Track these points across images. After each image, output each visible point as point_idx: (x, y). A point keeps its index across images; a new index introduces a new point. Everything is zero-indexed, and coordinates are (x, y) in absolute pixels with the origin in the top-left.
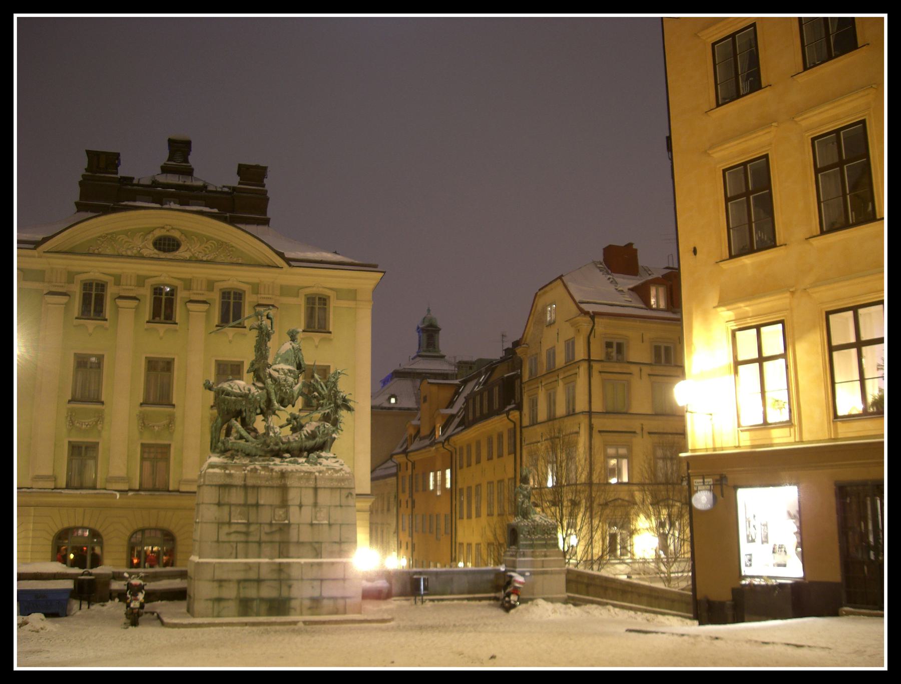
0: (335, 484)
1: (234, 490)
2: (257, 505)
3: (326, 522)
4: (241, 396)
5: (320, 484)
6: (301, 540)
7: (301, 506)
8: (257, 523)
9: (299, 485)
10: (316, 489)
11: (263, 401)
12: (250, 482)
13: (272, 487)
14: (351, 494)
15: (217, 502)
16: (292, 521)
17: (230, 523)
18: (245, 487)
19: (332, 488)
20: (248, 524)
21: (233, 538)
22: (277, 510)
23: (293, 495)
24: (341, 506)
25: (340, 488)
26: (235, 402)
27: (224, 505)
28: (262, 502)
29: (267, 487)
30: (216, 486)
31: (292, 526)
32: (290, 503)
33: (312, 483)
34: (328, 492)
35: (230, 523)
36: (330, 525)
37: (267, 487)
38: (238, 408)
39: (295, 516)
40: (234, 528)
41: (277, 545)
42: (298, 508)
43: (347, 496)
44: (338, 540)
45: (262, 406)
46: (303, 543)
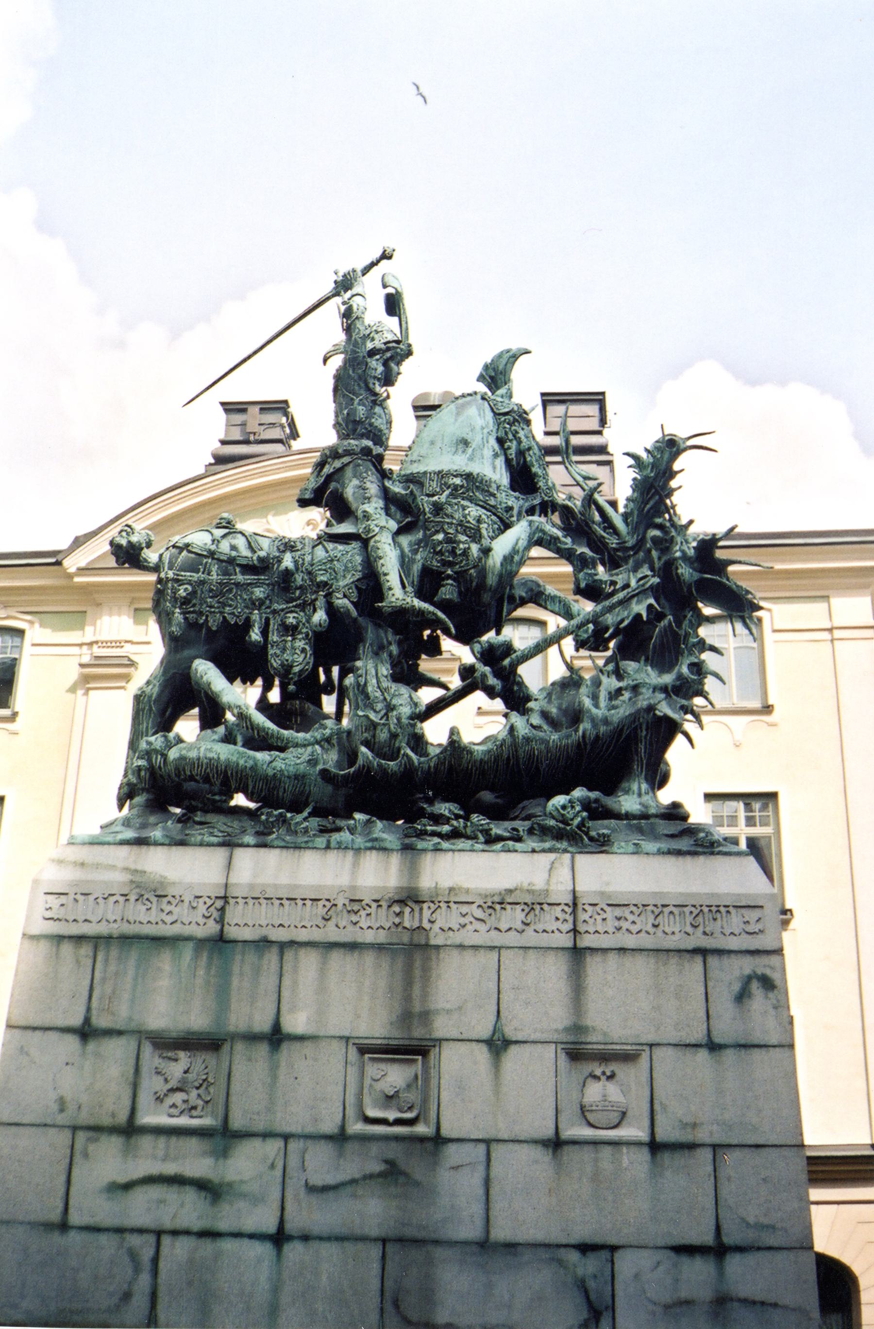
1: (165, 961)
2: (276, 1037)
3: (642, 1135)
4: (248, 569)
6: (501, 1232)
7: (498, 1044)
9: (497, 939)
11: (345, 581)
12: (243, 924)
15: (76, 1020)
17: (130, 1130)
21: (141, 1208)
22: (373, 1070)
23: (459, 993)
25: (703, 952)
26: (221, 592)
30: (79, 939)
33: (554, 930)
38: (234, 612)
39: (466, 1093)
40: (150, 1158)
41: (375, 1252)
42: (482, 1054)
44: (707, 1238)
45: (340, 602)
46: (511, 1247)
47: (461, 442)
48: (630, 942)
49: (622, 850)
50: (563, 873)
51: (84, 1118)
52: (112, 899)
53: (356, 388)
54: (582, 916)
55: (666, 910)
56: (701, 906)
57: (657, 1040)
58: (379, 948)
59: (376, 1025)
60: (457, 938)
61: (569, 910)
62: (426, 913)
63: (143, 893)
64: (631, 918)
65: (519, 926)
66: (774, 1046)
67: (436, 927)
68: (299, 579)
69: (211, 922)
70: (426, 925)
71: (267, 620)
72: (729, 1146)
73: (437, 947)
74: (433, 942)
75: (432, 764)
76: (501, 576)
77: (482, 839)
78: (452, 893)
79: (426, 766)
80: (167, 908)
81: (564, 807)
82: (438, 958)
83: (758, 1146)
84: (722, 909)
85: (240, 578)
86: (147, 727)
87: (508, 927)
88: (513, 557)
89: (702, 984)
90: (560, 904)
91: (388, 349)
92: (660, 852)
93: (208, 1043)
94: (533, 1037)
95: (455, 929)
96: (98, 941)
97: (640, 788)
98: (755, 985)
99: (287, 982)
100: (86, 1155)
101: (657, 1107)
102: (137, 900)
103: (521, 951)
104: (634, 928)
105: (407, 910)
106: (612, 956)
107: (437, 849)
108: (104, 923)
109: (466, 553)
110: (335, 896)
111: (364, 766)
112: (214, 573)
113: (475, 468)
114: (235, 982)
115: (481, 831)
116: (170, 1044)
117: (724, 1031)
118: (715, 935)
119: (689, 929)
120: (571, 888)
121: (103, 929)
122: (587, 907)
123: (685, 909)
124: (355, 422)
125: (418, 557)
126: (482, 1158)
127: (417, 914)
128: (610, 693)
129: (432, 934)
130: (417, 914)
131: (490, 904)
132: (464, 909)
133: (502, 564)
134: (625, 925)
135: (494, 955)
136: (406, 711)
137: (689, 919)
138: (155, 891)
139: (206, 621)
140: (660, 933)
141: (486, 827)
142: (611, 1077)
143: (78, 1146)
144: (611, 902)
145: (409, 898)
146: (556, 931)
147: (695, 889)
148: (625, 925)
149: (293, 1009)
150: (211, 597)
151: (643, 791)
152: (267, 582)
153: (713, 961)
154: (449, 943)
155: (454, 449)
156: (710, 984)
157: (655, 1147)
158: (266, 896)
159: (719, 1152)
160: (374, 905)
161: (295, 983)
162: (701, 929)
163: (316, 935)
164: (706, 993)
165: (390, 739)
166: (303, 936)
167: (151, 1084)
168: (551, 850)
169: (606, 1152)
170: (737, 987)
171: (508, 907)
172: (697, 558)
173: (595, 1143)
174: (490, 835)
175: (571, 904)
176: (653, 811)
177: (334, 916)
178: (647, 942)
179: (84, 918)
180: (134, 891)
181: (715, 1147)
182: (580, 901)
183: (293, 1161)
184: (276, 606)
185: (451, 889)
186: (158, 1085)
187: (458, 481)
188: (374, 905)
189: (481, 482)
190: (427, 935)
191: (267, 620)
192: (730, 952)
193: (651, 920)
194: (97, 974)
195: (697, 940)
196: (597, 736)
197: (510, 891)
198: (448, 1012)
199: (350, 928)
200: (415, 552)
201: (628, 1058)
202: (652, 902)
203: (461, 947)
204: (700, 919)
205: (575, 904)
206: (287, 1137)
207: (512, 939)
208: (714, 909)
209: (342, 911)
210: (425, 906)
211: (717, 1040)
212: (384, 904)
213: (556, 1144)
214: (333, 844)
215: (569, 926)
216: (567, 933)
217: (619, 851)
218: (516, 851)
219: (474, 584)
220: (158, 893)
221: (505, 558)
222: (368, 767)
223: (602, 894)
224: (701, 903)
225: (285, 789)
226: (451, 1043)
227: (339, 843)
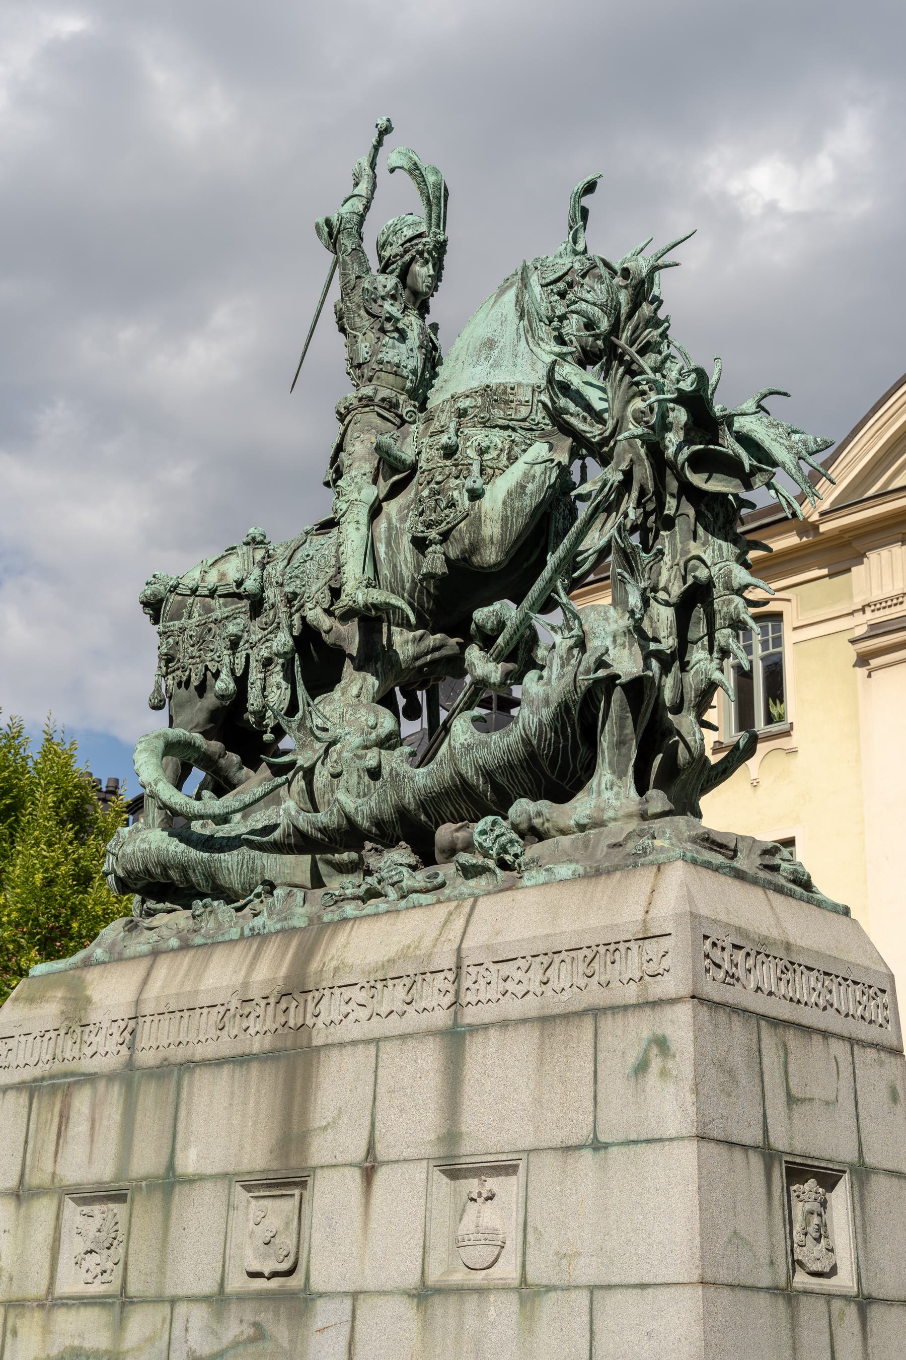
0: (567, 987)
2: (169, 1183)
5: (485, 999)
8: (158, 1300)
9: (377, 1028)
10: (455, 1038)
13: (241, 1060)
14: (662, 1044)
16: (318, 1283)
18: (129, 1076)
19: (545, 1020)
20: (120, 1303)
24: (598, 1146)
25: (596, 1012)
27: (38, 1192)
28: (190, 1161)
29: (219, 1062)
30: (19, 1087)
31: (328, 1313)
32: (320, 1151)
34: (524, 1041)
35: (51, 1303)
36: (528, 1292)
37: (219, 1062)
43: (641, 1068)
47: (485, 344)
48: (513, 1008)
49: (533, 882)
50: (458, 924)
51: (16, 1293)
52: (48, 1036)
53: (357, 320)
54: (467, 982)
55: (557, 959)
56: (598, 946)
57: (536, 1144)
58: (266, 1057)
59: (256, 1157)
60: (338, 1034)
61: (451, 976)
62: (311, 1005)
63: (70, 1024)
64: (518, 975)
65: (399, 1006)
66: (672, 1140)
67: (320, 1022)
68: (272, 594)
69: (124, 1050)
70: (310, 1021)
71: (248, 657)
72: (609, 1287)
73: (319, 1048)
74: (315, 1043)
75: (373, 804)
76: (505, 519)
77: (392, 894)
78: (337, 975)
79: (366, 809)
80: (92, 1038)
81: (483, 832)
82: (318, 1062)
83: (643, 1286)
84: (622, 947)
85: (217, 614)
86: (153, 818)
87: (389, 1010)
88: (523, 487)
89: (591, 1058)
90: (443, 971)
91: (406, 252)
92: (577, 877)
93: (114, 1195)
94: (406, 1154)
95: (337, 1022)
96: (32, 1088)
97: (599, 784)
98: (655, 1050)
99: (183, 1113)
100: (15, 1333)
101: (530, 1238)
102: (67, 1034)
103: (399, 1042)
104: (520, 990)
105: (294, 1004)
106: (493, 1033)
107: (345, 920)
108: (40, 1064)
109: (452, 504)
110: (229, 999)
111: (288, 826)
112: (196, 614)
113: (498, 378)
114: (139, 1117)
115: (393, 885)
116: (90, 1196)
117: (616, 1121)
118: (610, 986)
119: (582, 981)
120: (456, 946)
121: (37, 1072)
122: (470, 969)
123: (580, 954)
124: (359, 366)
125: (408, 524)
126: (348, 1316)
127: (301, 1008)
128: (561, 658)
129: (314, 1032)
130: (301, 1008)
131: (372, 983)
132: (348, 993)
133: (504, 503)
134: (510, 986)
135: (372, 1048)
136: (356, 740)
137: (582, 967)
138: (80, 1020)
139: (189, 676)
140: (549, 993)
141: (396, 879)
142: (490, 1198)
143: (10, 1325)
144: (496, 959)
145: (296, 988)
146: (437, 1008)
147: (592, 923)
148: (510, 986)
149: (186, 1147)
150: (193, 646)
151: (603, 786)
152: (244, 610)
153: (607, 1023)
154: (329, 1041)
155: (475, 359)
156: (601, 1057)
157: (528, 1292)
158: (170, 1010)
159: (598, 1294)
160: (263, 1003)
161: (189, 1114)
162: (596, 978)
163: (208, 1051)
164: (595, 1072)
165: (331, 782)
166: (200, 1052)
167: (72, 1246)
168: (449, 900)
169: (471, 1303)
170: (632, 1059)
171: (390, 983)
172: (693, 422)
173: (460, 1291)
174: (401, 888)
175: (454, 969)
176: (610, 814)
177: (227, 1025)
178: (531, 1007)
179: (25, 1062)
180: (64, 1025)
181: (592, 1289)
182: (467, 962)
183: (178, 1331)
184: (254, 638)
185: (336, 969)
186: (80, 1245)
187: (464, 404)
188: (263, 1003)
189: (505, 392)
190: (310, 1033)
191: (248, 657)
192: (625, 1008)
193: (536, 974)
194: (32, 1127)
195: (595, 996)
196: (540, 721)
197: (391, 961)
198: (325, 1128)
199: (241, 1036)
200: (403, 519)
201: (507, 1169)
202: (541, 948)
203: (342, 1045)
204: (595, 964)
205: (459, 967)
206: (173, 1301)
207: (393, 1026)
208: (612, 947)
209: (235, 1015)
210: (310, 997)
211: (602, 1138)
212: (272, 1000)
213: (424, 1294)
214: (247, 932)
215: (450, 998)
216: (449, 1008)
217: (528, 883)
218: (421, 905)
219: (467, 541)
220: (84, 1023)
221: (509, 493)
222: (294, 826)
223: (488, 947)
224: (597, 942)
225: (228, 869)
226: (326, 1172)
227: (252, 929)
